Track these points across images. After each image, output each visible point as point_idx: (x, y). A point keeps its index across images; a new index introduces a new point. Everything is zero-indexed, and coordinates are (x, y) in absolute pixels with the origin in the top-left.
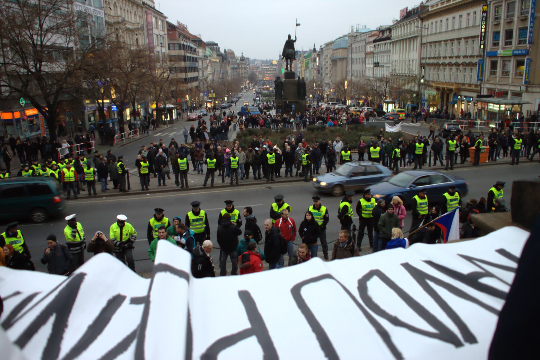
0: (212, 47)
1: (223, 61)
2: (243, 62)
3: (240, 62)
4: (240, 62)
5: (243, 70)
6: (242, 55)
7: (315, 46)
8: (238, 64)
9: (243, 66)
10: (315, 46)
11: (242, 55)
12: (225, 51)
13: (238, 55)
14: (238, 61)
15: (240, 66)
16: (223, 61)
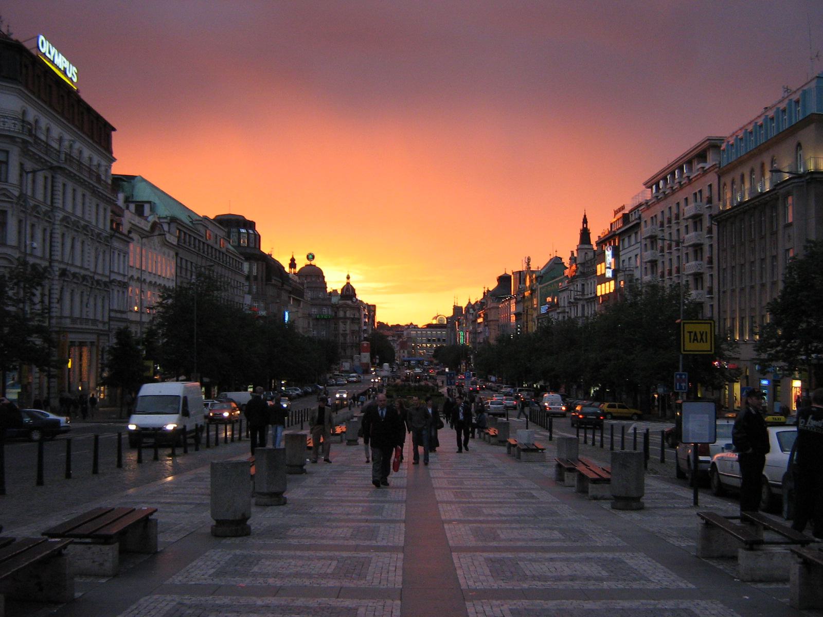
0: (234, 230)
1: (268, 279)
2: (349, 302)
3: (341, 302)
4: (341, 302)
5: (349, 322)
6: (348, 284)
7: (585, 221)
8: (336, 307)
9: (349, 314)
10: (585, 221)
11: (348, 284)
12: (293, 264)
13: (334, 282)
14: (334, 300)
15: (341, 314)
16: (268, 279)
